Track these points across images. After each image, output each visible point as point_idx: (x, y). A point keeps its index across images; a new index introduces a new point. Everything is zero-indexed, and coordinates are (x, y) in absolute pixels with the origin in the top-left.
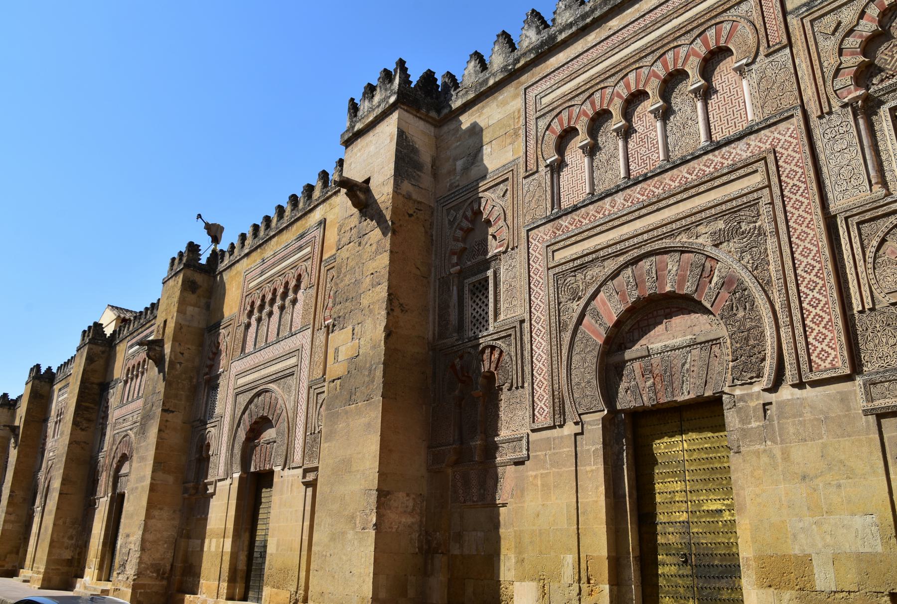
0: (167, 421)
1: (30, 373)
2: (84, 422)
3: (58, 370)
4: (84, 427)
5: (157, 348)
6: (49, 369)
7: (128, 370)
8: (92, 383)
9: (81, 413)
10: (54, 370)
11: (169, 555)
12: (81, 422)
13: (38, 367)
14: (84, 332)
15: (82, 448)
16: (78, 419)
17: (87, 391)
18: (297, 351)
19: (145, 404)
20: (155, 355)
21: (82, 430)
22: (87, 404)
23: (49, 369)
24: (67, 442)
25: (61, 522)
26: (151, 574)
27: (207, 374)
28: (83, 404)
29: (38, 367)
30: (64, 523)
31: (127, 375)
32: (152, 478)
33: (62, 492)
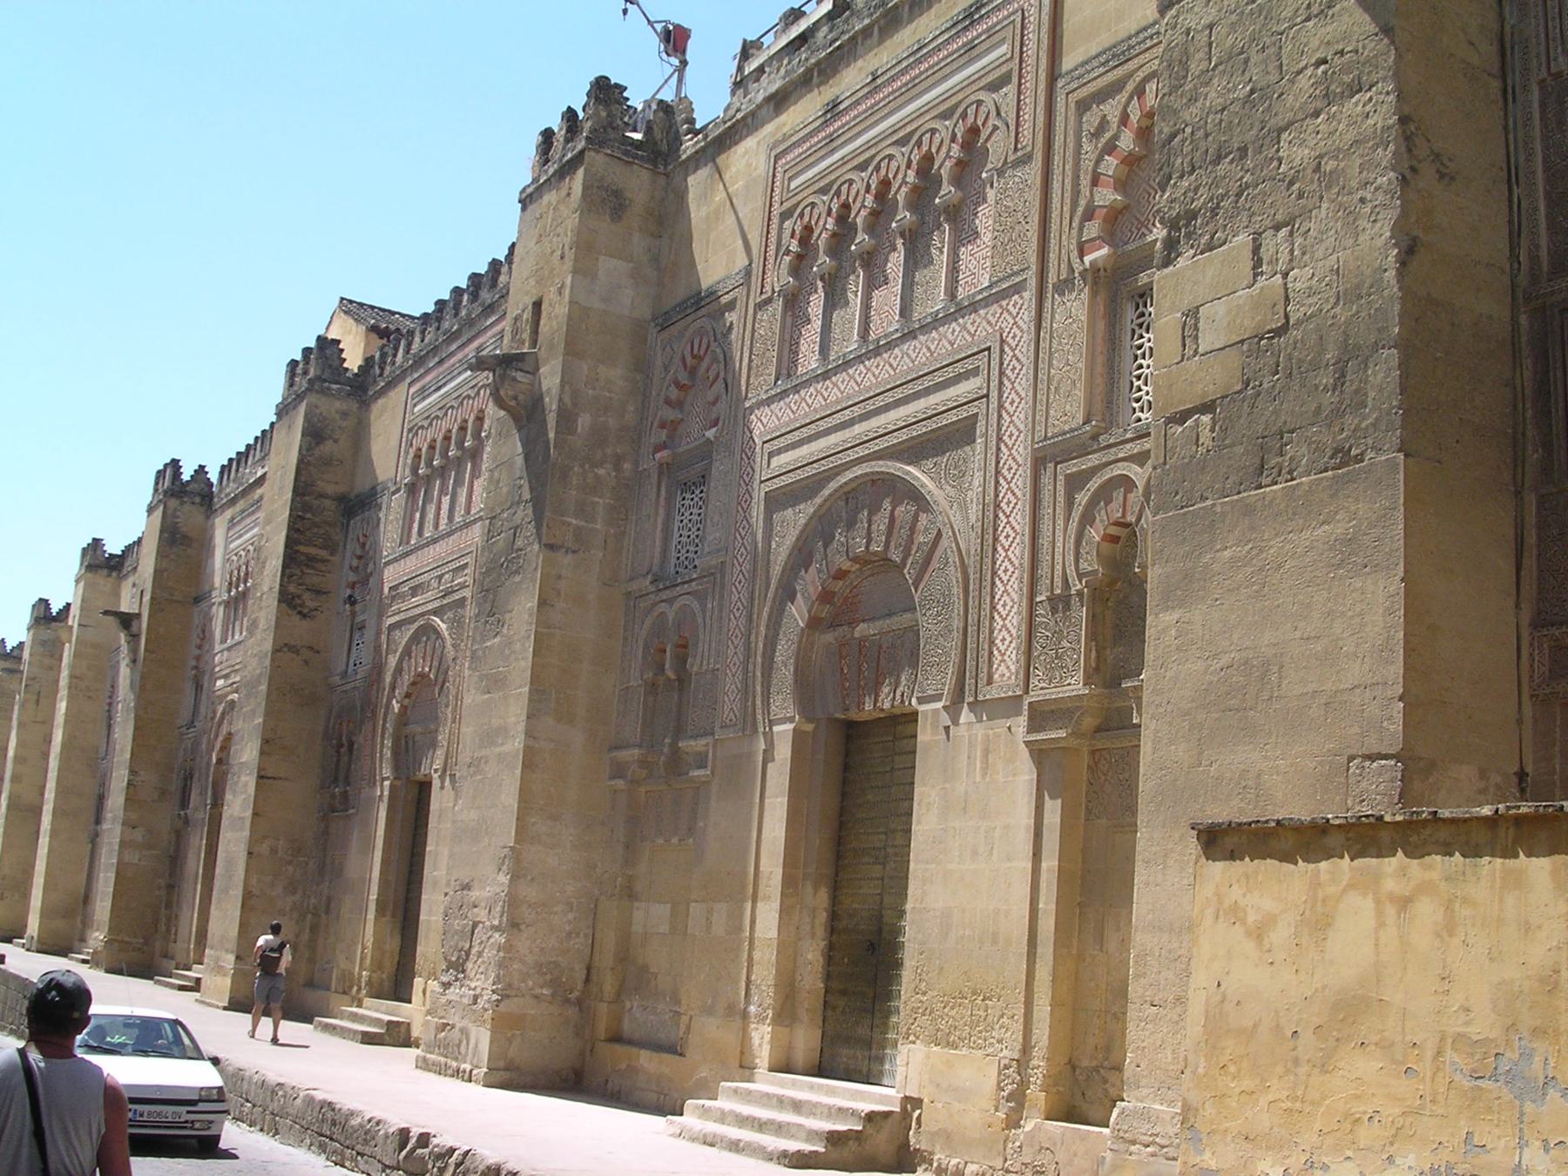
0: (560, 577)
1: (157, 483)
2: (307, 596)
3: (222, 473)
4: (306, 611)
5: (519, 376)
6: (201, 470)
7: (418, 456)
8: (321, 496)
9: (298, 572)
10: (213, 476)
11: (580, 943)
12: (299, 597)
13: (175, 464)
14: (293, 364)
15: (306, 662)
16: (292, 588)
17: (308, 515)
18: (990, 352)
19: (489, 535)
20: (515, 398)
21: (304, 616)
22: (312, 551)
23: (201, 470)
24: (268, 646)
25: (264, 848)
26: (538, 991)
27: (662, 447)
28: (302, 548)
29: (175, 464)
30: (274, 851)
31: (415, 470)
32: (529, 734)
33: (262, 773)
